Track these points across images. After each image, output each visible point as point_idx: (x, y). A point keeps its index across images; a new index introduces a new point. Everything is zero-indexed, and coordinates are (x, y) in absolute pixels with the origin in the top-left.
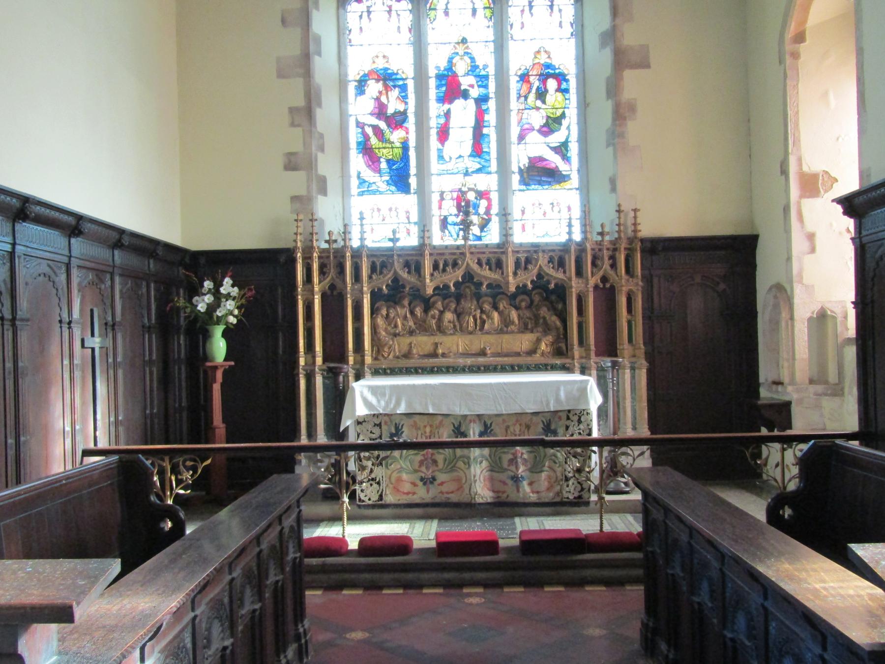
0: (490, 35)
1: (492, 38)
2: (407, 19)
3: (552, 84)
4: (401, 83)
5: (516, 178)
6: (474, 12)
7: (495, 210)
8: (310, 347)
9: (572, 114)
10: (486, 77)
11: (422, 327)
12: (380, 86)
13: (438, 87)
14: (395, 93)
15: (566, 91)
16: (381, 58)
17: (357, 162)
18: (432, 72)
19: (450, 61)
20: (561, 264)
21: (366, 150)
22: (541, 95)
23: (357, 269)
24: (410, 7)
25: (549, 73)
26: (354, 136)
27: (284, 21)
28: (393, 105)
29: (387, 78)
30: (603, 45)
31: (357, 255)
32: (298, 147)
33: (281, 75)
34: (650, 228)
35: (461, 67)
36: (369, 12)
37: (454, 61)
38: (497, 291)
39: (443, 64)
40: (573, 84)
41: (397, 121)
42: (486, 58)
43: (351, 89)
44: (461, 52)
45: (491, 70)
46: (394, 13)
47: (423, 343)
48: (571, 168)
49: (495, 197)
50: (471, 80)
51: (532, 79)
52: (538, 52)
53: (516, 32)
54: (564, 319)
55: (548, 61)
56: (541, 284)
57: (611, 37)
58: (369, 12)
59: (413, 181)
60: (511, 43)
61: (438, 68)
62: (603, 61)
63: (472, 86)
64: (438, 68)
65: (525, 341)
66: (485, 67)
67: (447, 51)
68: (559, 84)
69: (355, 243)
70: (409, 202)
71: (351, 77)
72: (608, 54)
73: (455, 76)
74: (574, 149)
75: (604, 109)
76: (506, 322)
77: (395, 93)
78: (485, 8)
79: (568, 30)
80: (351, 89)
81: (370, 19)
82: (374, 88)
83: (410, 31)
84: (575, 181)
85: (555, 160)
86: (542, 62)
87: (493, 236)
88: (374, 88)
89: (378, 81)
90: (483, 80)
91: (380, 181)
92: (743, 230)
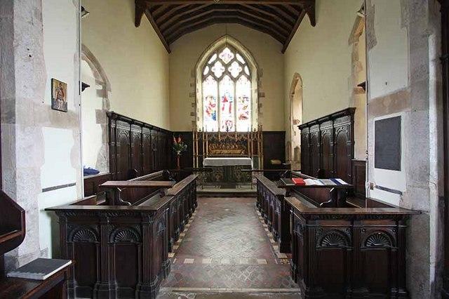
5: (238, 119)
7: (234, 124)
8: (196, 151)
9: (249, 106)
11: (218, 148)
17: (205, 114)
20: (246, 136)
21: (207, 112)
22: (243, 102)
23: (205, 136)
26: (205, 109)
27: (191, 86)
28: (213, 102)
31: (205, 133)
32: (194, 111)
34: (264, 130)
35: (227, 96)
38: (234, 141)
41: (213, 106)
47: (219, 151)
48: (249, 116)
49: (234, 121)
54: (247, 147)
56: (242, 140)
57: (258, 90)
59: (217, 118)
62: (255, 96)
65: (239, 151)
69: (205, 131)
70: (216, 122)
72: (256, 94)
74: (250, 113)
75: (256, 105)
76: (235, 147)
82: (209, 99)
84: (250, 119)
85: (246, 115)
88: (209, 99)
91: (210, 118)
92: (283, 130)
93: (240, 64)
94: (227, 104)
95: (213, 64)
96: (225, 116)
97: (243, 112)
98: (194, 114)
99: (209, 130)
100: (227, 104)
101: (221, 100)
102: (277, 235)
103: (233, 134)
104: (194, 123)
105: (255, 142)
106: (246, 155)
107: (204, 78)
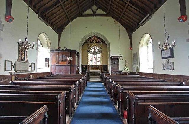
48: (100, 61)
57: (102, 56)
75: (101, 59)
87: (96, 64)
93: (98, 49)
94: (95, 58)
95: (92, 49)
96: (94, 61)
97: (98, 60)
98: (88, 61)
99: (91, 64)
100: (95, 58)
101: (94, 57)
102: (102, 78)
103: (96, 65)
104: (88, 63)
105: (101, 67)
106: (99, 70)
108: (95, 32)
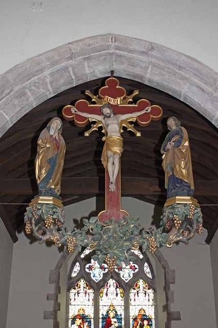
0: (122, 303)
1: (123, 304)
2: (92, 296)
3: (146, 322)
4: (89, 320)
6: (117, 295)
10: (121, 319)
12: (81, 321)
13: (102, 322)
14: (87, 324)
15: (152, 325)
16: (82, 310)
18: (101, 316)
19: (108, 312)
24: (93, 291)
25: (144, 318)
27: (48, 298)
29: (84, 318)
30: (164, 311)
33: (45, 318)
35: (112, 315)
36: (78, 293)
37: (109, 312)
39: (105, 313)
40: (153, 322)
42: (121, 311)
43: (70, 322)
44: (112, 309)
45: (123, 316)
46: (87, 294)
50: (115, 320)
51: (138, 320)
52: (141, 310)
53: (132, 302)
55: (144, 313)
57: (166, 308)
58: (78, 293)
60: (130, 306)
61: (103, 315)
63: (115, 322)
64: (103, 315)
66: (121, 315)
67: (106, 308)
68: (148, 322)
71: (70, 317)
73: (109, 318)
77: (87, 324)
78: (121, 293)
79: (151, 302)
80: (70, 322)
81: (78, 296)
82: (78, 322)
83: (93, 300)
86: (142, 314)
88: (78, 322)
89: (80, 319)
90: (119, 320)
107: (72, 284)
108: (116, 38)
